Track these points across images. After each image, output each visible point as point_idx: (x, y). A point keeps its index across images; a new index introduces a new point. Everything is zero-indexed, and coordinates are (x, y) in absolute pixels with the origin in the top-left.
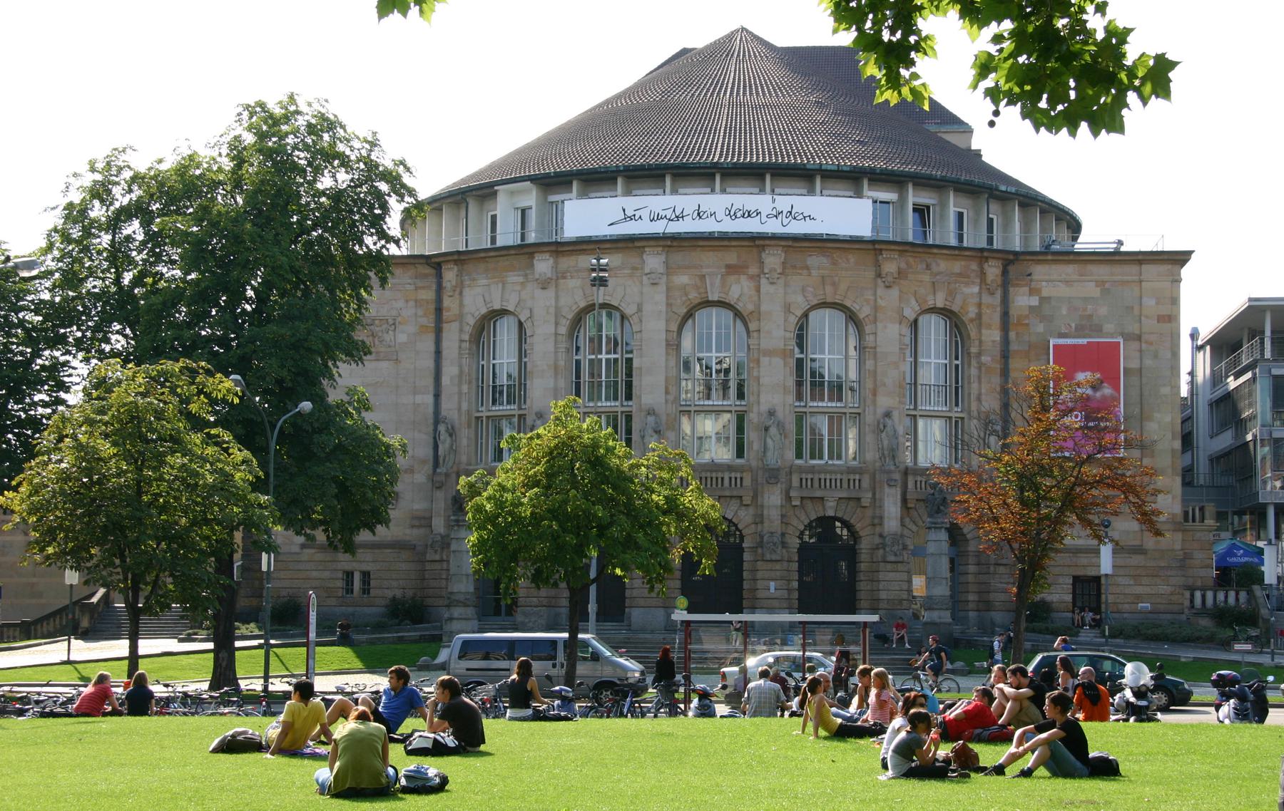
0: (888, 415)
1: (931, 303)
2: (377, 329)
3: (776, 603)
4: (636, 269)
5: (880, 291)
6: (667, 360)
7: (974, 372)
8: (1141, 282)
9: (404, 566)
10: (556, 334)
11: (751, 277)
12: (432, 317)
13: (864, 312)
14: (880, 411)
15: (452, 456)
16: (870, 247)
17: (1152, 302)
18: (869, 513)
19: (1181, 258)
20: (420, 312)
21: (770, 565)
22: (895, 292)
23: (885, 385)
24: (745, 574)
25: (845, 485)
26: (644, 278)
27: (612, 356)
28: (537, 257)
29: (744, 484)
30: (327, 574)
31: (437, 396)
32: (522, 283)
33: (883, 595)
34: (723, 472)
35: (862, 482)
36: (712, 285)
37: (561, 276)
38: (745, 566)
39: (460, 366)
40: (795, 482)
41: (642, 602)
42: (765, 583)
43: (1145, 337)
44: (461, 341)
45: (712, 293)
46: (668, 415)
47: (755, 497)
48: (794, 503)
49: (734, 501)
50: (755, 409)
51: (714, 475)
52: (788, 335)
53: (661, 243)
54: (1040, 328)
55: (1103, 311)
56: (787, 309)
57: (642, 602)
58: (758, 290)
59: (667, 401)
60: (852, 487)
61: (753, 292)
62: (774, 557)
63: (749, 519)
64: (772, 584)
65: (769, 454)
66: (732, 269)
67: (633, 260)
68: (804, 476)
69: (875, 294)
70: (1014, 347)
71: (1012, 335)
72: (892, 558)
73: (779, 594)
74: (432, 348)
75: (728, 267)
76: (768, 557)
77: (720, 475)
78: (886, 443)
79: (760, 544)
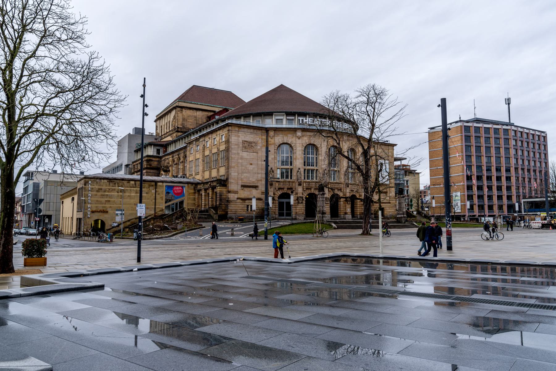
8: (389, 149)
9: (260, 204)
12: (266, 143)
19: (396, 145)
27: (308, 156)
28: (298, 131)
30: (243, 206)
32: (292, 137)
37: (303, 136)
44: (275, 149)
64: (349, 209)
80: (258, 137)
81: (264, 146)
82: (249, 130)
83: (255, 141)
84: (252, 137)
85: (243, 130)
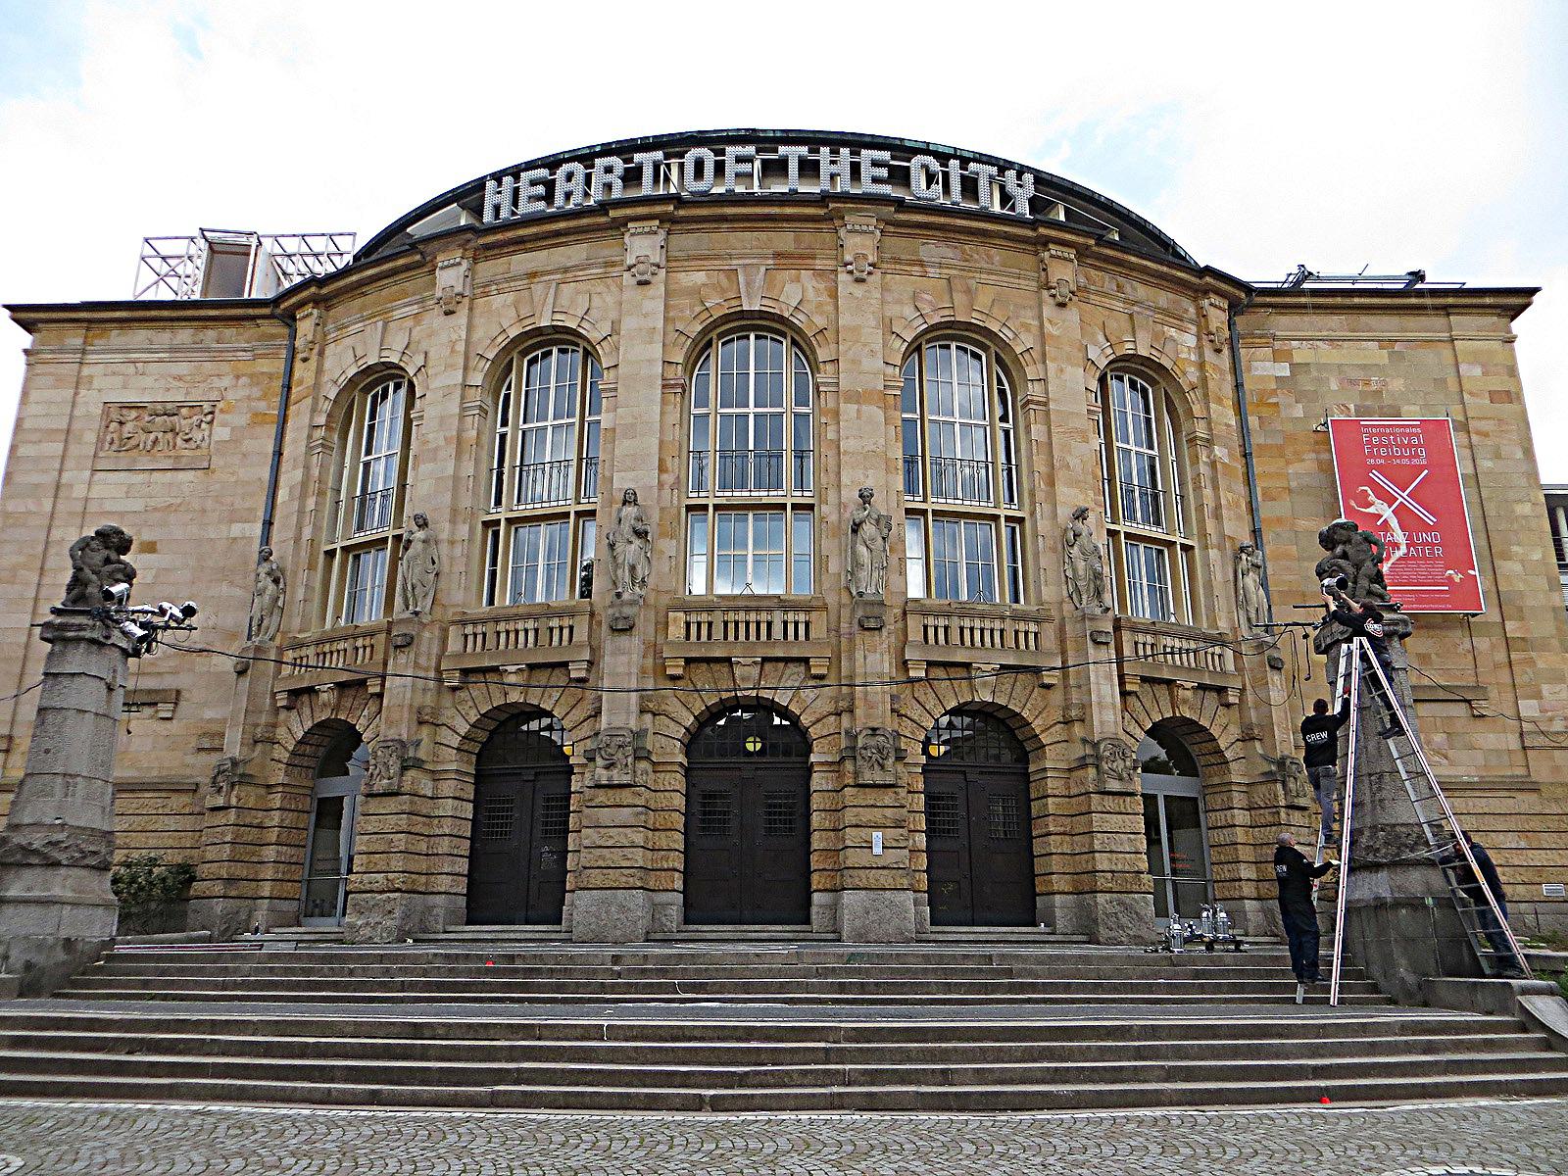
0: (1081, 515)
1: (1127, 349)
2: (183, 422)
3: (885, 878)
4: (613, 264)
5: (1048, 310)
6: (662, 413)
7: (1203, 469)
9: (172, 823)
10: (465, 386)
11: (819, 273)
12: (277, 400)
13: (1023, 342)
14: (1064, 513)
15: (275, 618)
16: (1030, 233)
17: (1477, 371)
18: (1056, 697)
19: (1514, 301)
20: (256, 392)
21: (871, 797)
22: (1072, 315)
23: (1068, 467)
24: (816, 819)
25: (1010, 642)
26: (626, 275)
29: (812, 635)
31: (268, 524)
33: (1102, 862)
34: (769, 610)
35: (1042, 638)
36: (748, 284)
38: (816, 801)
39: (307, 467)
40: (914, 635)
41: (596, 878)
42: (863, 833)
43: (1472, 424)
45: (749, 295)
46: (662, 509)
47: (835, 660)
48: (912, 674)
49: (792, 668)
50: (832, 496)
51: (753, 617)
52: (890, 370)
53: (658, 209)
54: (1298, 411)
55: (1397, 385)
56: (889, 330)
57: (596, 878)
58: (834, 295)
59: (661, 485)
60: (1022, 646)
61: (825, 298)
62: (878, 777)
63: (824, 706)
64: (877, 836)
65: (863, 575)
66: (783, 259)
67: (606, 249)
68: (931, 621)
69: (1040, 317)
70: (1257, 439)
71: (1253, 421)
72: (1114, 785)
73: (892, 857)
74: (270, 448)
75: (777, 255)
76: (868, 777)
77: (764, 617)
78: (1081, 565)
79: (851, 753)
80: (225, 367)
81: (258, 419)
82: (164, 338)
83: (196, 395)
84: (179, 378)
85: (116, 338)
